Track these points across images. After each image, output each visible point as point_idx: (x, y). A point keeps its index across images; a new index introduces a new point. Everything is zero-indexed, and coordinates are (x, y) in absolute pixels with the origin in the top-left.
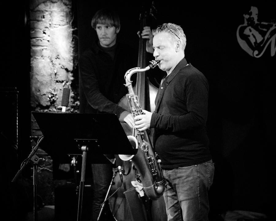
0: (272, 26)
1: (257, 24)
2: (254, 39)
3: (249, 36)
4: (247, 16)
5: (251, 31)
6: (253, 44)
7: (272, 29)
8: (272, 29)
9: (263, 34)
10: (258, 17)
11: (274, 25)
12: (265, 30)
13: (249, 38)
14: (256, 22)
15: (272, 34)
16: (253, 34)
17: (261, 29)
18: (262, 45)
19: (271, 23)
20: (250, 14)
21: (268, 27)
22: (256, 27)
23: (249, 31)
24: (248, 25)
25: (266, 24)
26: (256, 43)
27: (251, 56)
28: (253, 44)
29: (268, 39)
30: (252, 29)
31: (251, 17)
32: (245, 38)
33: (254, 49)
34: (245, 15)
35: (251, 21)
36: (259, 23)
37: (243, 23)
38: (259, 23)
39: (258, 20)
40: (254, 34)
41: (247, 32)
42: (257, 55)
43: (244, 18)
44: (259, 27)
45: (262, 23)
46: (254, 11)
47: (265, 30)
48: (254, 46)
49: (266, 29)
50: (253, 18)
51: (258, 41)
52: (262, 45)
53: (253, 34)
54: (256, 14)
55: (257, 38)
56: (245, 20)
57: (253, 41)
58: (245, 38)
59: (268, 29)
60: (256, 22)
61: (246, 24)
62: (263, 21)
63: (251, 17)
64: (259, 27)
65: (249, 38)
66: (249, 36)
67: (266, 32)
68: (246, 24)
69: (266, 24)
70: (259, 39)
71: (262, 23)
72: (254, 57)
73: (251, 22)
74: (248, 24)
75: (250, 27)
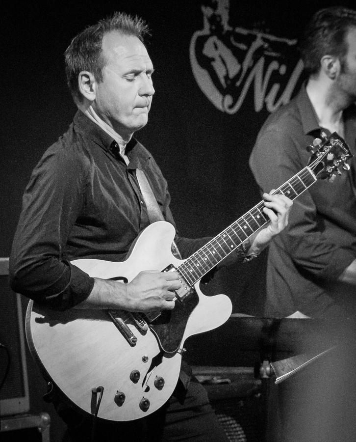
0: (254, 38)
1: (228, 31)
2: (223, 68)
3: (213, 60)
4: (207, 11)
5: (216, 47)
6: (223, 81)
9: (240, 56)
10: (230, 14)
11: (259, 35)
12: (243, 47)
13: (214, 64)
14: (227, 27)
15: (255, 60)
16: (220, 56)
17: (234, 43)
18: (238, 84)
19: (254, 32)
20: (214, 6)
21: (249, 40)
22: (225, 39)
23: (213, 46)
24: (213, 33)
25: (243, 31)
26: (227, 77)
27: (219, 111)
28: (223, 81)
29: (249, 70)
30: (219, 43)
31: (218, 12)
32: (206, 63)
33: (223, 92)
34: (206, 6)
35: (215, 20)
36: (231, 29)
37: (201, 27)
38: (231, 29)
39: (230, 23)
40: (223, 55)
41: (208, 50)
42: (231, 107)
43: (201, 14)
44: (232, 39)
45: (239, 30)
47: (243, 47)
48: (225, 86)
49: (245, 44)
50: (219, 16)
51: (232, 75)
52: (238, 84)
53: (220, 56)
54: (226, 8)
55: (228, 67)
56: (206, 21)
57: (221, 73)
58: (206, 63)
59: (249, 45)
60: (227, 27)
61: (206, 31)
62: (239, 26)
63: (218, 12)
64: (232, 39)
65: (214, 64)
66: (213, 60)
67: (246, 52)
68: (206, 31)
69: (243, 31)
70: (234, 69)
71: (239, 30)
72: (225, 113)
73: (217, 30)
74: (211, 29)
75: (214, 39)
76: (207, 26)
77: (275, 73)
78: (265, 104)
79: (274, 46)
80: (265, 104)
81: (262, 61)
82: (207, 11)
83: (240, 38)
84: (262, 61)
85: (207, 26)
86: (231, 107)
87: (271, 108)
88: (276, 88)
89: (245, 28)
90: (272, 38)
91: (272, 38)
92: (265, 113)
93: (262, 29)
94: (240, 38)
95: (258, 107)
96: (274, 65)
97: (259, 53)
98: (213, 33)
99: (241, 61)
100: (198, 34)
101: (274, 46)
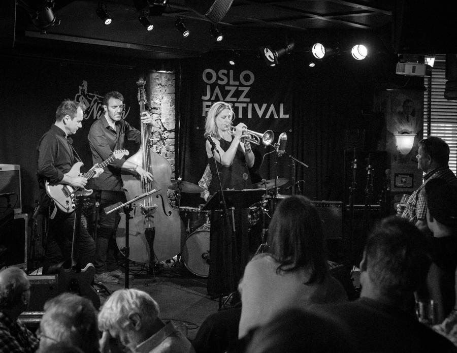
7: (95, 98)
8: (95, 98)
11: (96, 96)
12: (91, 99)
14: (86, 93)
15: (94, 103)
19: (95, 95)
20: (83, 86)
25: (92, 94)
29: (93, 106)
30: (84, 97)
35: (83, 91)
37: (79, 93)
42: (86, 117)
45: (90, 94)
46: (85, 83)
47: (91, 99)
59: (93, 99)
60: (86, 93)
61: (80, 94)
67: (91, 101)
68: (80, 94)
69: (92, 94)
71: (90, 94)
73: (83, 94)
76: (80, 92)
77: (100, 107)
78: (97, 117)
79: (100, 99)
80: (97, 117)
81: (96, 104)
82: (81, 88)
83: (90, 96)
84: (96, 104)
85: (80, 92)
86: (86, 117)
87: (98, 118)
88: (100, 111)
89: (92, 93)
90: (100, 97)
91: (100, 97)
92: (96, 119)
93: (97, 94)
94: (90, 96)
95: (94, 118)
96: (100, 105)
97: (96, 101)
98: (82, 94)
99: (90, 103)
100: (78, 94)
101: (100, 99)
